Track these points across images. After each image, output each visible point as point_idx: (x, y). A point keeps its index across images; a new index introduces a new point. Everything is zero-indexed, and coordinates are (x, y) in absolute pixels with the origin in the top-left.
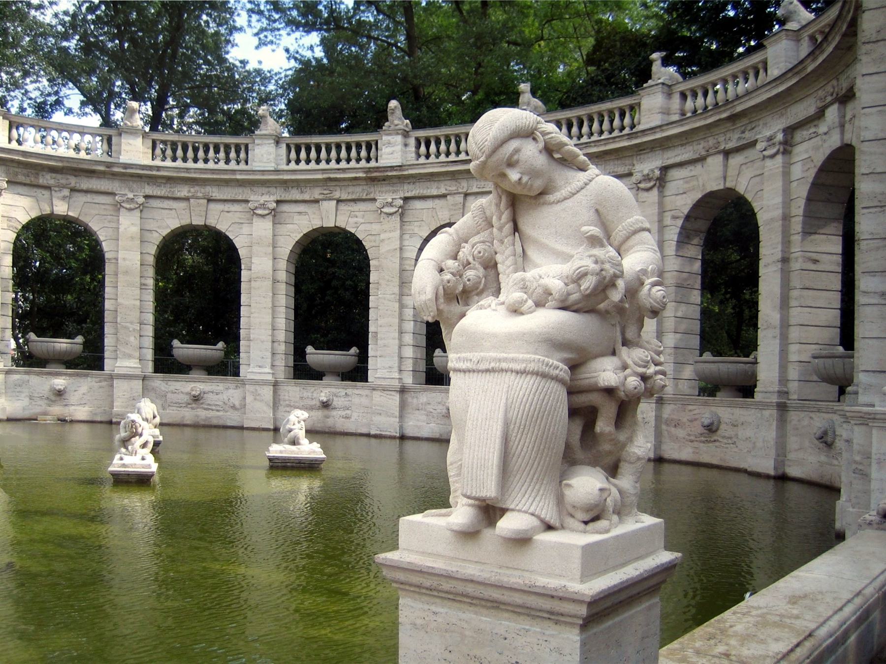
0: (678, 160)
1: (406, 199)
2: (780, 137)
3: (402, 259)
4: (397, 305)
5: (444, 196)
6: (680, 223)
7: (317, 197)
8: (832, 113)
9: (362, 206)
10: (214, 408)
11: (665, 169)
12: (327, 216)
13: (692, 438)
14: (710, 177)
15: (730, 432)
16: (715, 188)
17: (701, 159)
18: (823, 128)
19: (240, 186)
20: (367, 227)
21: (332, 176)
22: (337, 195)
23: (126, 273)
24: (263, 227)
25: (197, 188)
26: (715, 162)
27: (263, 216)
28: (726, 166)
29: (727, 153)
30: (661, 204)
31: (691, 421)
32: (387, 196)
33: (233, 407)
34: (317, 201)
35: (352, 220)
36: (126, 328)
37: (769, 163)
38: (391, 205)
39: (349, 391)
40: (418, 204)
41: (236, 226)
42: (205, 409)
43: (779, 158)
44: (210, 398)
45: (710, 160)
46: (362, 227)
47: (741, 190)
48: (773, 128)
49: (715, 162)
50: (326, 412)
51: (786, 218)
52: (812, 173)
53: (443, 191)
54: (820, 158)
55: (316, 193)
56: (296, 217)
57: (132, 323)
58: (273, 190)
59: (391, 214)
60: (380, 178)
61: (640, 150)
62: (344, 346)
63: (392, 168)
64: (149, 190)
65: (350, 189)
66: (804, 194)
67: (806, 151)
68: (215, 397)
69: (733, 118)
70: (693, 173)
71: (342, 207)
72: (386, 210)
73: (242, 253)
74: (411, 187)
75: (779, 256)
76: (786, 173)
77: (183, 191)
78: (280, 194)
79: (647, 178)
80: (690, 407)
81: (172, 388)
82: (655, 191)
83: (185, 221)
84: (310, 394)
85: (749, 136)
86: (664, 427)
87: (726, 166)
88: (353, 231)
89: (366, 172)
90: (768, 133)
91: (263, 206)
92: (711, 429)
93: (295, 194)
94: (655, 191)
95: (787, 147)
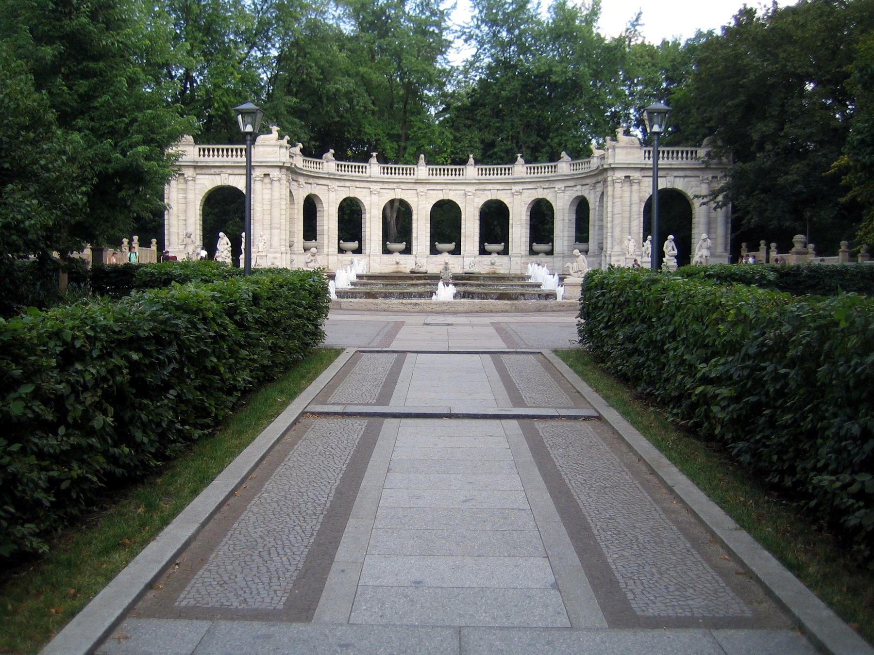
8: (579, 187)
12: (399, 194)
14: (540, 194)
18: (575, 189)
24: (375, 198)
32: (420, 188)
49: (540, 190)
55: (394, 186)
62: (497, 242)
77: (348, 184)
85: (552, 186)
93: (386, 186)
95: (564, 191)
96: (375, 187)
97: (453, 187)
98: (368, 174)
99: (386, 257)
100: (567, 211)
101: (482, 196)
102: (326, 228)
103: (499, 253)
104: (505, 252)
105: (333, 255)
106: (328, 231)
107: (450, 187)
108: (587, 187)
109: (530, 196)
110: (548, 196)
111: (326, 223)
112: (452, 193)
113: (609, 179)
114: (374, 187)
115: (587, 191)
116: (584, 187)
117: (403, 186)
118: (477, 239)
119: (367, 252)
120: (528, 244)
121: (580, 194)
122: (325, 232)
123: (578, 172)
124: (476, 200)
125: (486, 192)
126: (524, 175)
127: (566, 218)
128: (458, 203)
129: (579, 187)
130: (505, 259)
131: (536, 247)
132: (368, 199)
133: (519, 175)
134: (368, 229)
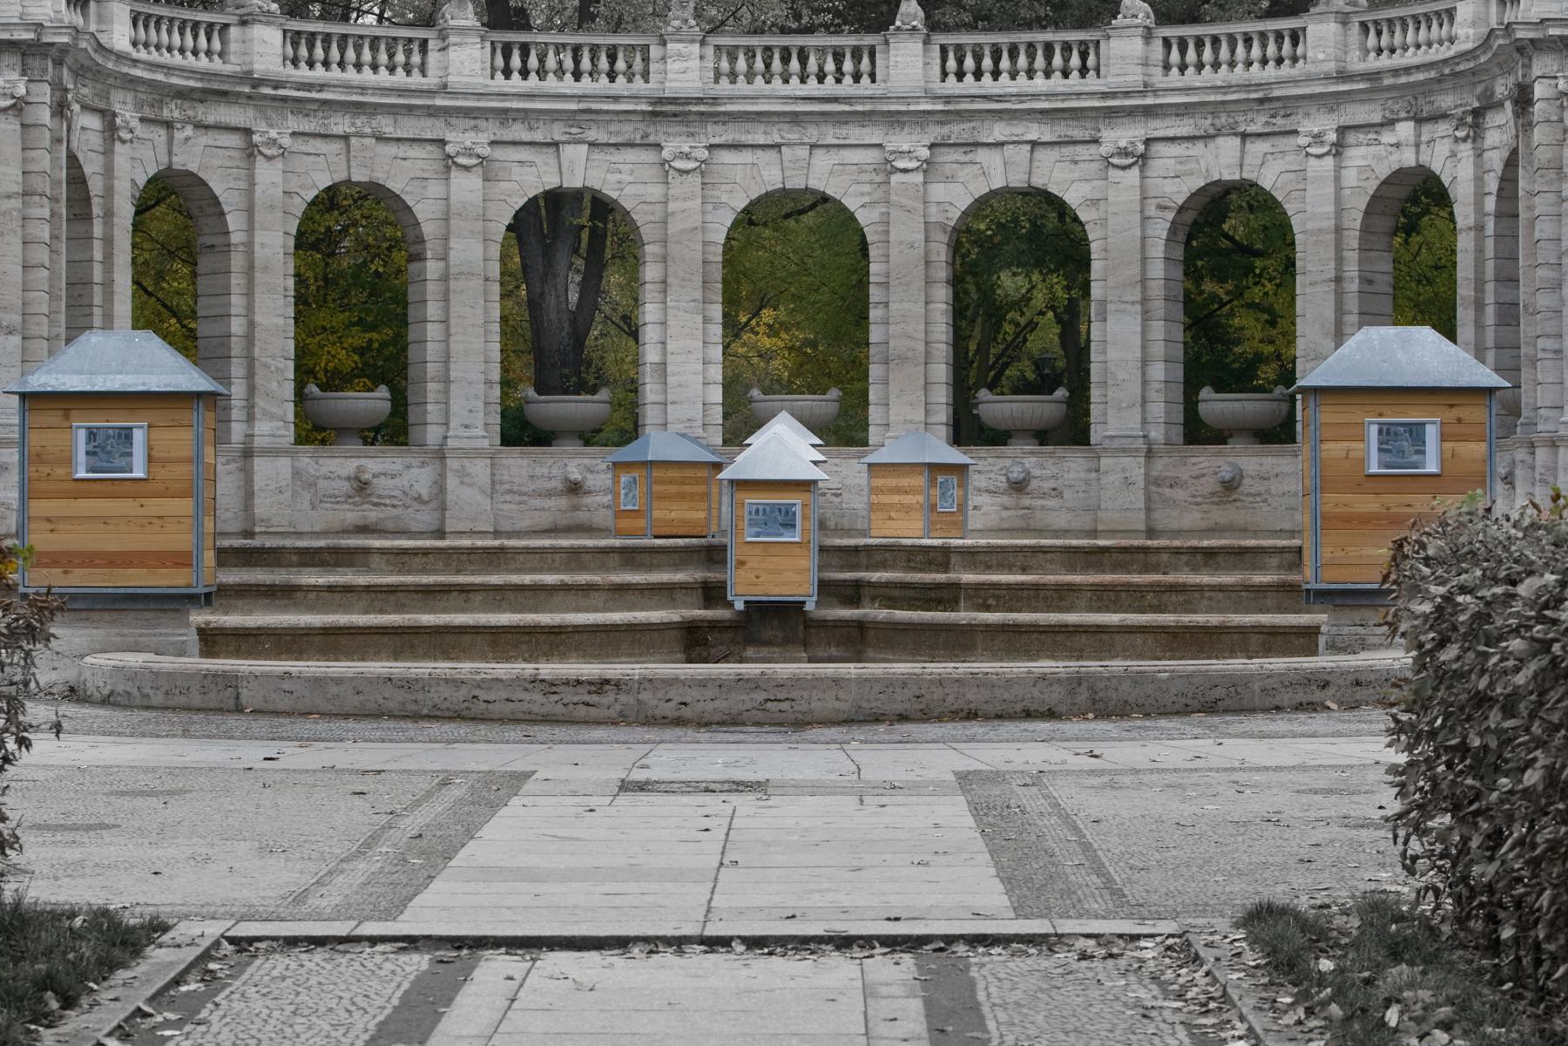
0: (1170, 133)
1: (711, 147)
2: (1333, 137)
3: (705, 243)
4: (700, 319)
5: (777, 147)
6: (1170, 215)
7: (557, 137)
8: (1405, 130)
9: (631, 155)
10: (387, 501)
11: (1148, 142)
12: (579, 168)
13: (1199, 500)
14: (1222, 161)
15: (1259, 487)
16: (1226, 177)
17: (1207, 137)
18: (1387, 137)
19: (430, 115)
20: (641, 189)
21: (594, 106)
22: (593, 134)
23: (266, 269)
26: (1229, 145)
27: (466, 168)
28: (1243, 151)
29: (1245, 136)
30: (1143, 188)
31: (1196, 478)
32: (675, 143)
33: (419, 499)
36: (266, 366)
37: (1312, 161)
38: (687, 157)
40: (727, 157)
41: (415, 183)
42: (375, 505)
43: (1329, 161)
44: (383, 485)
45: (1220, 140)
46: (629, 190)
47: (1267, 185)
48: (1324, 124)
50: (575, 500)
51: (1339, 230)
52: (1372, 185)
53: (776, 138)
54: (1384, 171)
55: (557, 132)
56: (516, 169)
57: (273, 357)
58: (482, 123)
59: (687, 172)
60: (669, 111)
61: (1111, 114)
63: (700, 101)
64: (295, 123)
65: (613, 128)
66: (1363, 207)
67: (1364, 157)
68: (390, 483)
69: (1261, 101)
70: (1190, 152)
71: (598, 156)
72: (678, 164)
73: (428, 229)
74: (719, 128)
75: (1332, 274)
76: (1337, 179)
78: (492, 130)
79: (1124, 153)
80: (1193, 460)
81: (324, 470)
82: (1135, 171)
83: (340, 176)
84: (546, 471)
86: (1154, 489)
87: (1243, 151)
89: (651, 104)
90: (1316, 130)
91: (469, 152)
92: (1230, 486)
93: (518, 132)
94: (1135, 171)
95: (1338, 149)
96: (469, 139)
97: (830, 135)
98: (432, 80)
99: (520, 464)
100: (1352, 239)
101: (964, 173)
102: (237, 326)
103: (1043, 436)
104: (1072, 430)
105: (273, 452)
106: (249, 338)
107: (813, 133)
108: (1444, 128)
109: (1183, 171)
110: (1270, 169)
111: (237, 302)
113: (1539, 90)
114: (460, 138)
115: (1443, 148)
116: (1427, 131)
119: (433, 434)
120: (1178, 394)
121: (1408, 158)
122: (236, 347)
123: (1398, 60)
125: (982, 155)
127: (1352, 269)
129: (1405, 130)
130: (1069, 465)
131: (1216, 405)
132: (435, 189)
133: (1134, 78)
134: (433, 331)
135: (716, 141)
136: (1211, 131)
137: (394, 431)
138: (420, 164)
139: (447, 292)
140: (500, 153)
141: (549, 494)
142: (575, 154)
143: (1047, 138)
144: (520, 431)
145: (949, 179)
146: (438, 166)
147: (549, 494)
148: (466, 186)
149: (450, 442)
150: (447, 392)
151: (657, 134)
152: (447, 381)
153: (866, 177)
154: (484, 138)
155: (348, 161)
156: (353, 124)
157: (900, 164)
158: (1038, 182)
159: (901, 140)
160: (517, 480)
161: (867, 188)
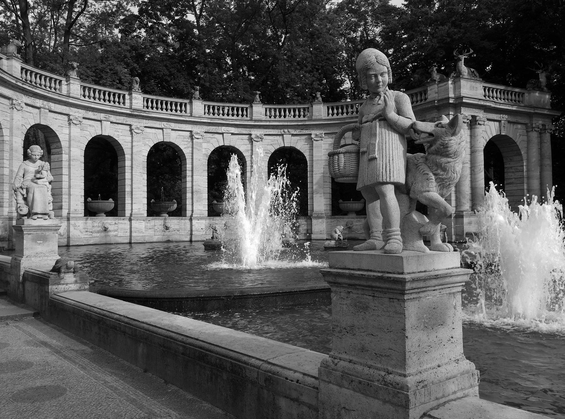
12: (108, 130)
25: (45, 103)
34: (100, 121)
35: (116, 133)
39: (117, 222)
41: (60, 128)
46: (121, 138)
55: (101, 116)
56: (89, 128)
77: (39, 103)
79: (257, 137)
88: (117, 139)
93: (90, 115)
96: (77, 115)
112: (174, 134)
117: (113, 118)
118: (205, 196)
124: (205, 145)
125: (216, 136)
126: (263, 117)
128: (182, 147)
135: (146, 125)
136: (283, 133)
137: (113, 213)
138: (61, 122)
139: (69, 165)
140: (85, 121)
141: (98, 232)
142: (106, 124)
143: (236, 132)
144: (90, 212)
145: (208, 142)
146: (67, 123)
147: (98, 232)
148: (75, 130)
149: (71, 215)
150: (69, 198)
151: (130, 121)
152: (70, 195)
153: (185, 140)
154: (81, 115)
155: (40, 117)
156: (43, 104)
157: (197, 137)
158: (232, 144)
159: (196, 129)
160: (89, 228)
161: (186, 143)
